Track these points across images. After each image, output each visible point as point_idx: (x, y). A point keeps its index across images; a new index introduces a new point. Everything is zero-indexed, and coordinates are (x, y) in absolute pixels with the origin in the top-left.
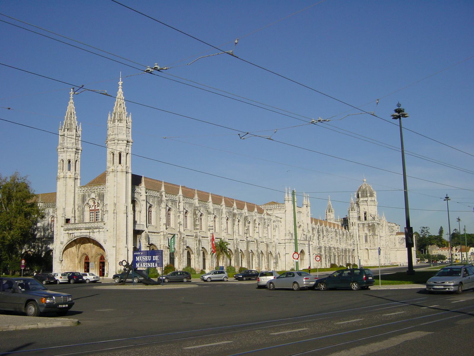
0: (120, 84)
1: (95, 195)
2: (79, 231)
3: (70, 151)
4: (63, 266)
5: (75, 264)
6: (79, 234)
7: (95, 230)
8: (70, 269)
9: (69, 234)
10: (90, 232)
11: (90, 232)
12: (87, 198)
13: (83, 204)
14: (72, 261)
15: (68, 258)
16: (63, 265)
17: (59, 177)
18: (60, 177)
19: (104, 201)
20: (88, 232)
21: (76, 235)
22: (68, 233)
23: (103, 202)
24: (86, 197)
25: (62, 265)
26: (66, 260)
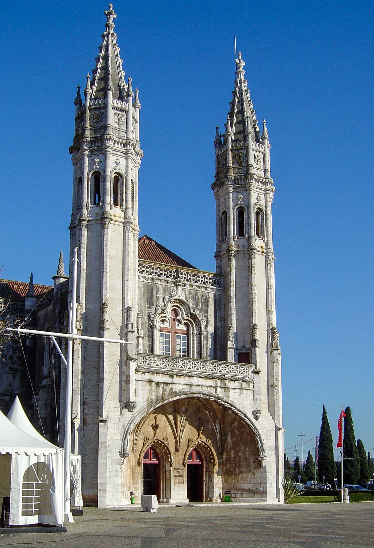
1: (183, 294)
2: (186, 380)
9: (153, 383)
10: (216, 388)
11: (216, 388)
12: (161, 295)
13: (149, 308)
18: (113, 218)
19: (208, 313)
20: (211, 386)
21: (176, 388)
22: (150, 381)
23: (207, 317)
24: (157, 292)
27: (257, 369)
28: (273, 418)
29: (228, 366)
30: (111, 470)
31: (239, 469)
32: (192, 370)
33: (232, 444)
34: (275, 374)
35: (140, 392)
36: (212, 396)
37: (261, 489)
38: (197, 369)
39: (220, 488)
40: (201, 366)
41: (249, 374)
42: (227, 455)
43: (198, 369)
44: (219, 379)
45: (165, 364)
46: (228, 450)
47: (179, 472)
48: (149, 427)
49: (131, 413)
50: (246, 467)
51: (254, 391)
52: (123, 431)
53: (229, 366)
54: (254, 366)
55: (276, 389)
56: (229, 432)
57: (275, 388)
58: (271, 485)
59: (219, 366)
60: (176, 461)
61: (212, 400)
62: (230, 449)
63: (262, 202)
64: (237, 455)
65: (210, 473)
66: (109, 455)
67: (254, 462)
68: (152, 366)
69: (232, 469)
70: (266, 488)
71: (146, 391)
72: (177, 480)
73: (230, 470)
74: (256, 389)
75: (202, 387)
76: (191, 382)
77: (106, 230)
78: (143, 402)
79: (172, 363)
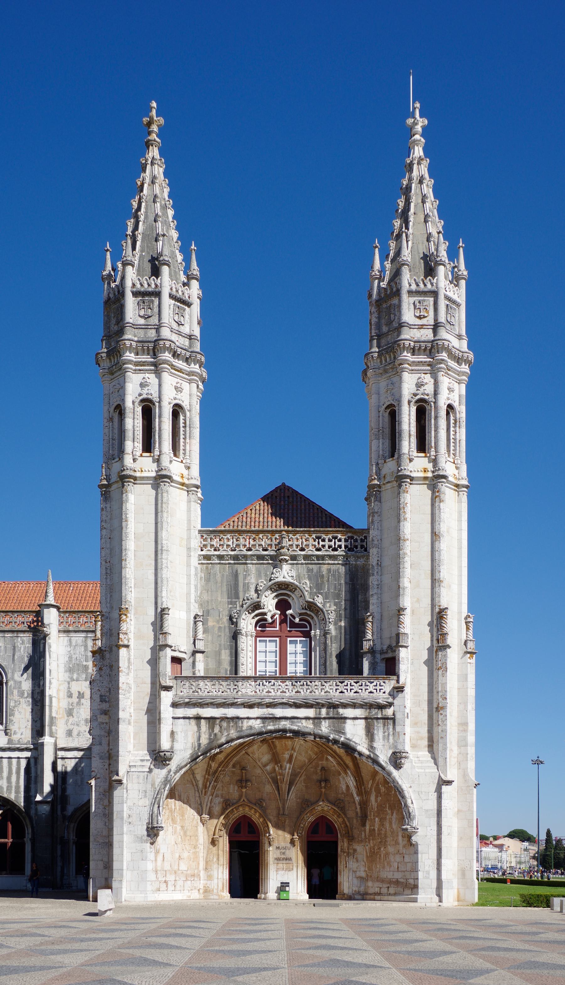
0: (419, 128)
3: (180, 371)
4: (160, 858)
5: (197, 850)
6: (257, 725)
8: (181, 868)
14: (188, 833)
15: (175, 824)
16: (162, 851)
17: (132, 473)
18: (138, 474)
20: (307, 718)
22: (198, 718)
25: (157, 852)
27: (401, 683)
28: (436, 764)
29: (342, 683)
34: (440, 689)
35: (179, 737)
37: (411, 881)
38: (283, 692)
40: (291, 688)
41: (384, 693)
43: (285, 692)
44: (323, 706)
45: (224, 689)
48: (232, 786)
51: (394, 720)
52: (153, 793)
53: (344, 682)
54: (395, 677)
55: (441, 714)
56: (371, 789)
57: (441, 712)
58: (429, 874)
59: (325, 684)
63: (429, 388)
65: (345, 854)
66: (130, 829)
67: (402, 837)
68: (200, 693)
69: (376, 848)
70: (418, 879)
71: (190, 734)
74: (398, 716)
77: (124, 495)
78: (185, 750)
79: (236, 687)
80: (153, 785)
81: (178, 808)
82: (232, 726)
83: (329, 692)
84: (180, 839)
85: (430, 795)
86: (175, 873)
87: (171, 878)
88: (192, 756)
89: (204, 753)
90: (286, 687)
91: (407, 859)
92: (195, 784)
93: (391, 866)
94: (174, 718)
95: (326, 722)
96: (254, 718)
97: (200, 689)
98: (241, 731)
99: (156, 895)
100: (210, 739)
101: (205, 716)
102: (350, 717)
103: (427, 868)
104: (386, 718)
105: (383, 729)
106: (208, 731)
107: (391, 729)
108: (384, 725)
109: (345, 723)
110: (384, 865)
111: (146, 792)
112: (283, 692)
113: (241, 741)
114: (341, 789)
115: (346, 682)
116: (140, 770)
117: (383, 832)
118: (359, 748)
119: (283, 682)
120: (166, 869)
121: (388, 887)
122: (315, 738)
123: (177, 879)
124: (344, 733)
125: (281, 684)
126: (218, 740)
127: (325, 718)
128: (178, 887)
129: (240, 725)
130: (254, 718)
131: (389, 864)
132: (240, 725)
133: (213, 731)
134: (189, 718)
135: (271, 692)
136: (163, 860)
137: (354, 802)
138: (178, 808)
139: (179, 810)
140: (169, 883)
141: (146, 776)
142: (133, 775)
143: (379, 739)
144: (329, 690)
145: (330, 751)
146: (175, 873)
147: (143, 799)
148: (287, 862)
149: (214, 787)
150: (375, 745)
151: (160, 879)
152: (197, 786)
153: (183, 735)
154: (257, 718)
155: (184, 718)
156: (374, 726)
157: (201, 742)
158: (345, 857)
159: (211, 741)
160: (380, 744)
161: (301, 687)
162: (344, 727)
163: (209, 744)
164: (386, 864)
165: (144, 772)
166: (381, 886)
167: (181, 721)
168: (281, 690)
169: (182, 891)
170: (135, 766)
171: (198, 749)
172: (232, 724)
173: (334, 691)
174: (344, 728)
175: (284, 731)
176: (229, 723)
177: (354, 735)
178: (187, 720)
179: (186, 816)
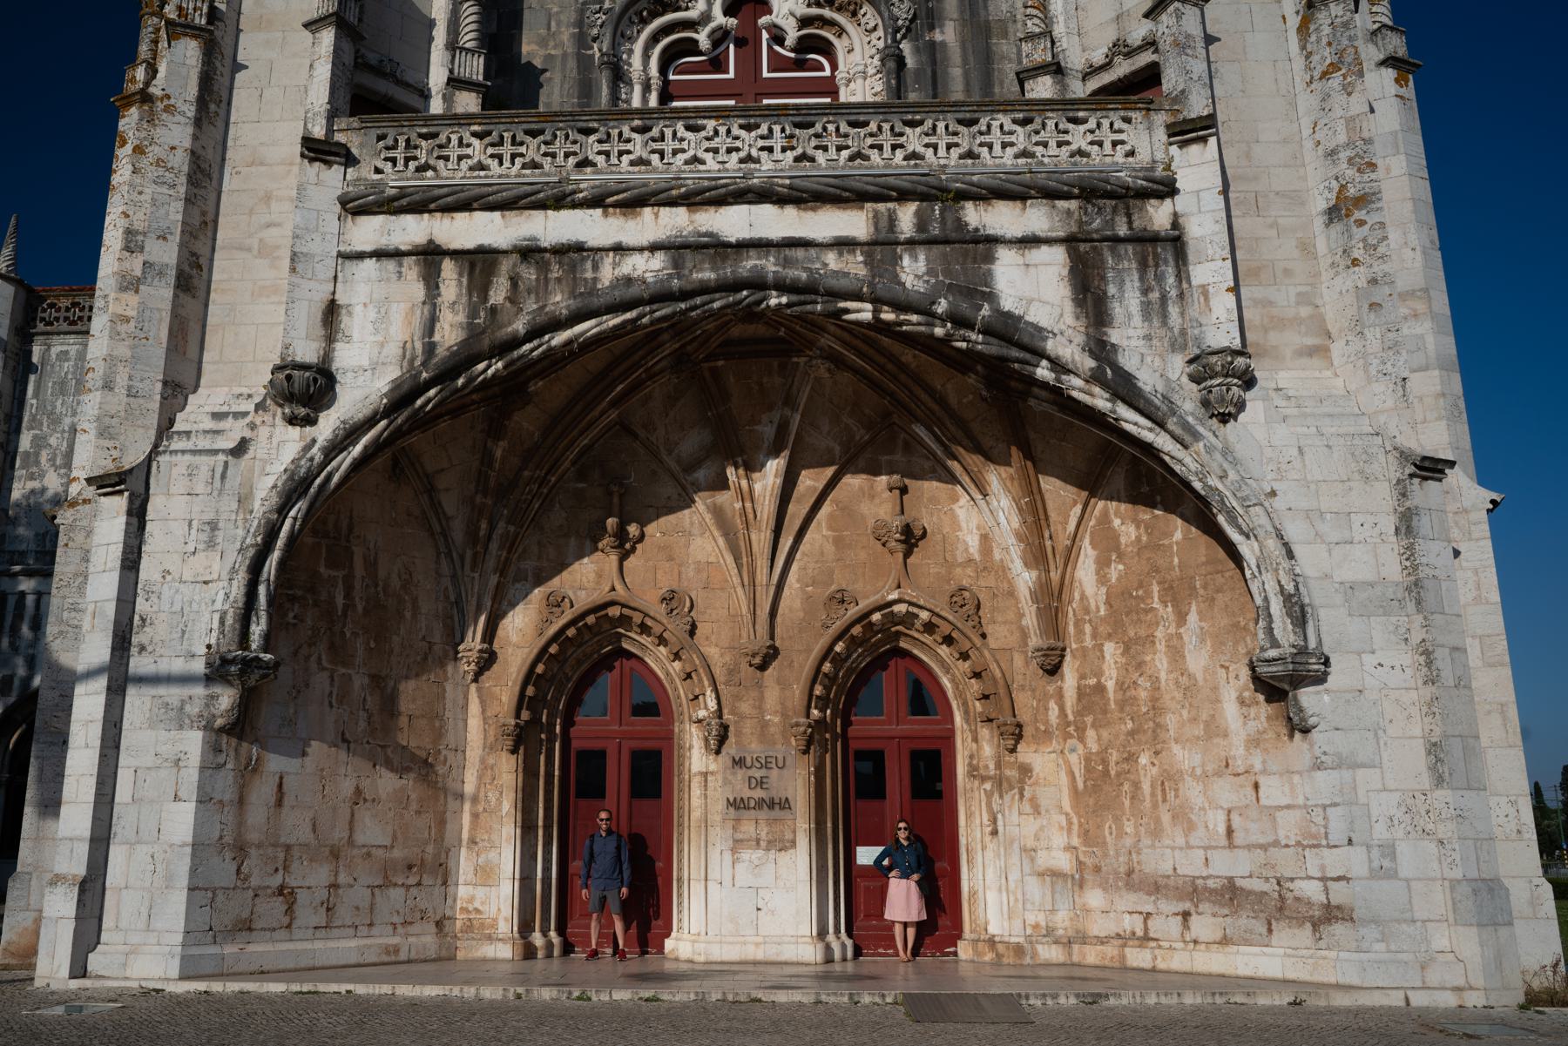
7: (1000, 218)
8: (360, 838)
9: (448, 268)
15: (345, 664)
20: (843, 244)
22: (430, 255)
26: (320, 681)
30: (149, 760)
31: (1157, 753)
32: (711, 163)
33: (1108, 603)
35: (358, 324)
36: (859, 297)
39: (1055, 874)
40: (778, 142)
42: (1082, 677)
43: (757, 161)
46: (1088, 642)
47: (761, 783)
49: (294, 432)
50: (1198, 738)
52: (240, 532)
59: (908, 130)
60: (742, 717)
61: (858, 323)
62: (1094, 636)
64: (1140, 665)
71: (398, 312)
72: (748, 829)
73: (1105, 762)
75: (787, 252)
76: (703, 229)
79: (576, 148)
80: (243, 500)
81: (360, 608)
82: (559, 280)
83: (922, 158)
84: (362, 725)
85: (1356, 526)
86: (335, 854)
87: (312, 877)
88: (397, 385)
89: (444, 376)
90: (761, 143)
91: (1273, 792)
92: (437, 528)
93: (1190, 827)
94: (341, 255)
95: (916, 259)
96: (641, 250)
97: (447, 159)
98: (593, 291)
99: (230, 949)
100: (470, 326)
101: (456, 244)
102: (1009, 236)
103: (1380, 832)
104: (1146, 240)
105: (1142, 279)
106: (464, 299)
107: (1171, 280)
108: (1143, 266)
109: (990, 258)
110: (1158, 821)
111: (213, 526)
112: (749, 159)
113: (587, 327)
114: (961, 547)
115: (983, 122)
116: (204, 443)
117: (1143, 694)
118: (1050, 346)
119: (748, 128)
120: (291, 840)
121: (1186, 915)
122: (876, 312)
123: (343, 878)
124: (991, 297)
125: (743, 133)
126: (500, 328)
127: (911, 243)
128: (344, 914)
129: (589, 275)
130: (641, 250)
131: (1182, 817)
132: (589, 275)
133: (485, 299)
134: (396, 254)
135: (703, 162)
136: (279, 803)
137: (1012, 593)
138: (360, 608)
139: (366, 612)
140: (302, 896)
141: (219, 470)
142: (173, 465)
143: (1130, 316)
144: (920, 149)
145: (924, 396)
146: (335, 854)
147: (201, 556)
148: (777, 813)
149: (511, 544)
150: (1114, 336)
151: (255, 881)
152: (445, 534)
153: (372, 314)
154: (654, 248)
155: (379, 254)
156: (1103, 262)
157: (437, 338)
158: (989, 795)
159: (473, 333)
160: (1131, 332)
161: (814, 142)
162: (989, 270)
163: (464, 344)
164: (1166, 818)
165: (215, 452)
166: (1149, 908)
167: (370, 264)
168: (742, 154)
169: (363, 930)
170: (188, 434)
171: (424, 364)
172: (555, 272)
173: (942, 152)
174: (987, 279)
175: (758, 284)
176: (543, 268)
177: (1030, 301)
178: (390, 265)
179: (396, 639)
